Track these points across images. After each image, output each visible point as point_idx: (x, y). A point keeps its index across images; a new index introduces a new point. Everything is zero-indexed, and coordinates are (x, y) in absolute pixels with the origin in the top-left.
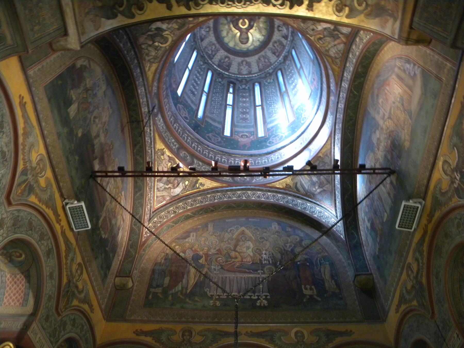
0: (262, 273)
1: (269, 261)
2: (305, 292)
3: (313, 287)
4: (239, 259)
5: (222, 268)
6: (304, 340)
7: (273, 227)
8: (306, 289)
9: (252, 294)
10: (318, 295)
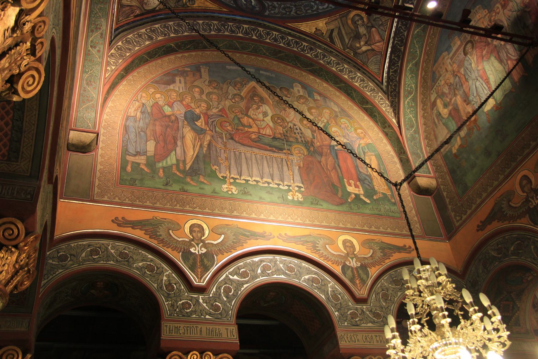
5: (232, 138)
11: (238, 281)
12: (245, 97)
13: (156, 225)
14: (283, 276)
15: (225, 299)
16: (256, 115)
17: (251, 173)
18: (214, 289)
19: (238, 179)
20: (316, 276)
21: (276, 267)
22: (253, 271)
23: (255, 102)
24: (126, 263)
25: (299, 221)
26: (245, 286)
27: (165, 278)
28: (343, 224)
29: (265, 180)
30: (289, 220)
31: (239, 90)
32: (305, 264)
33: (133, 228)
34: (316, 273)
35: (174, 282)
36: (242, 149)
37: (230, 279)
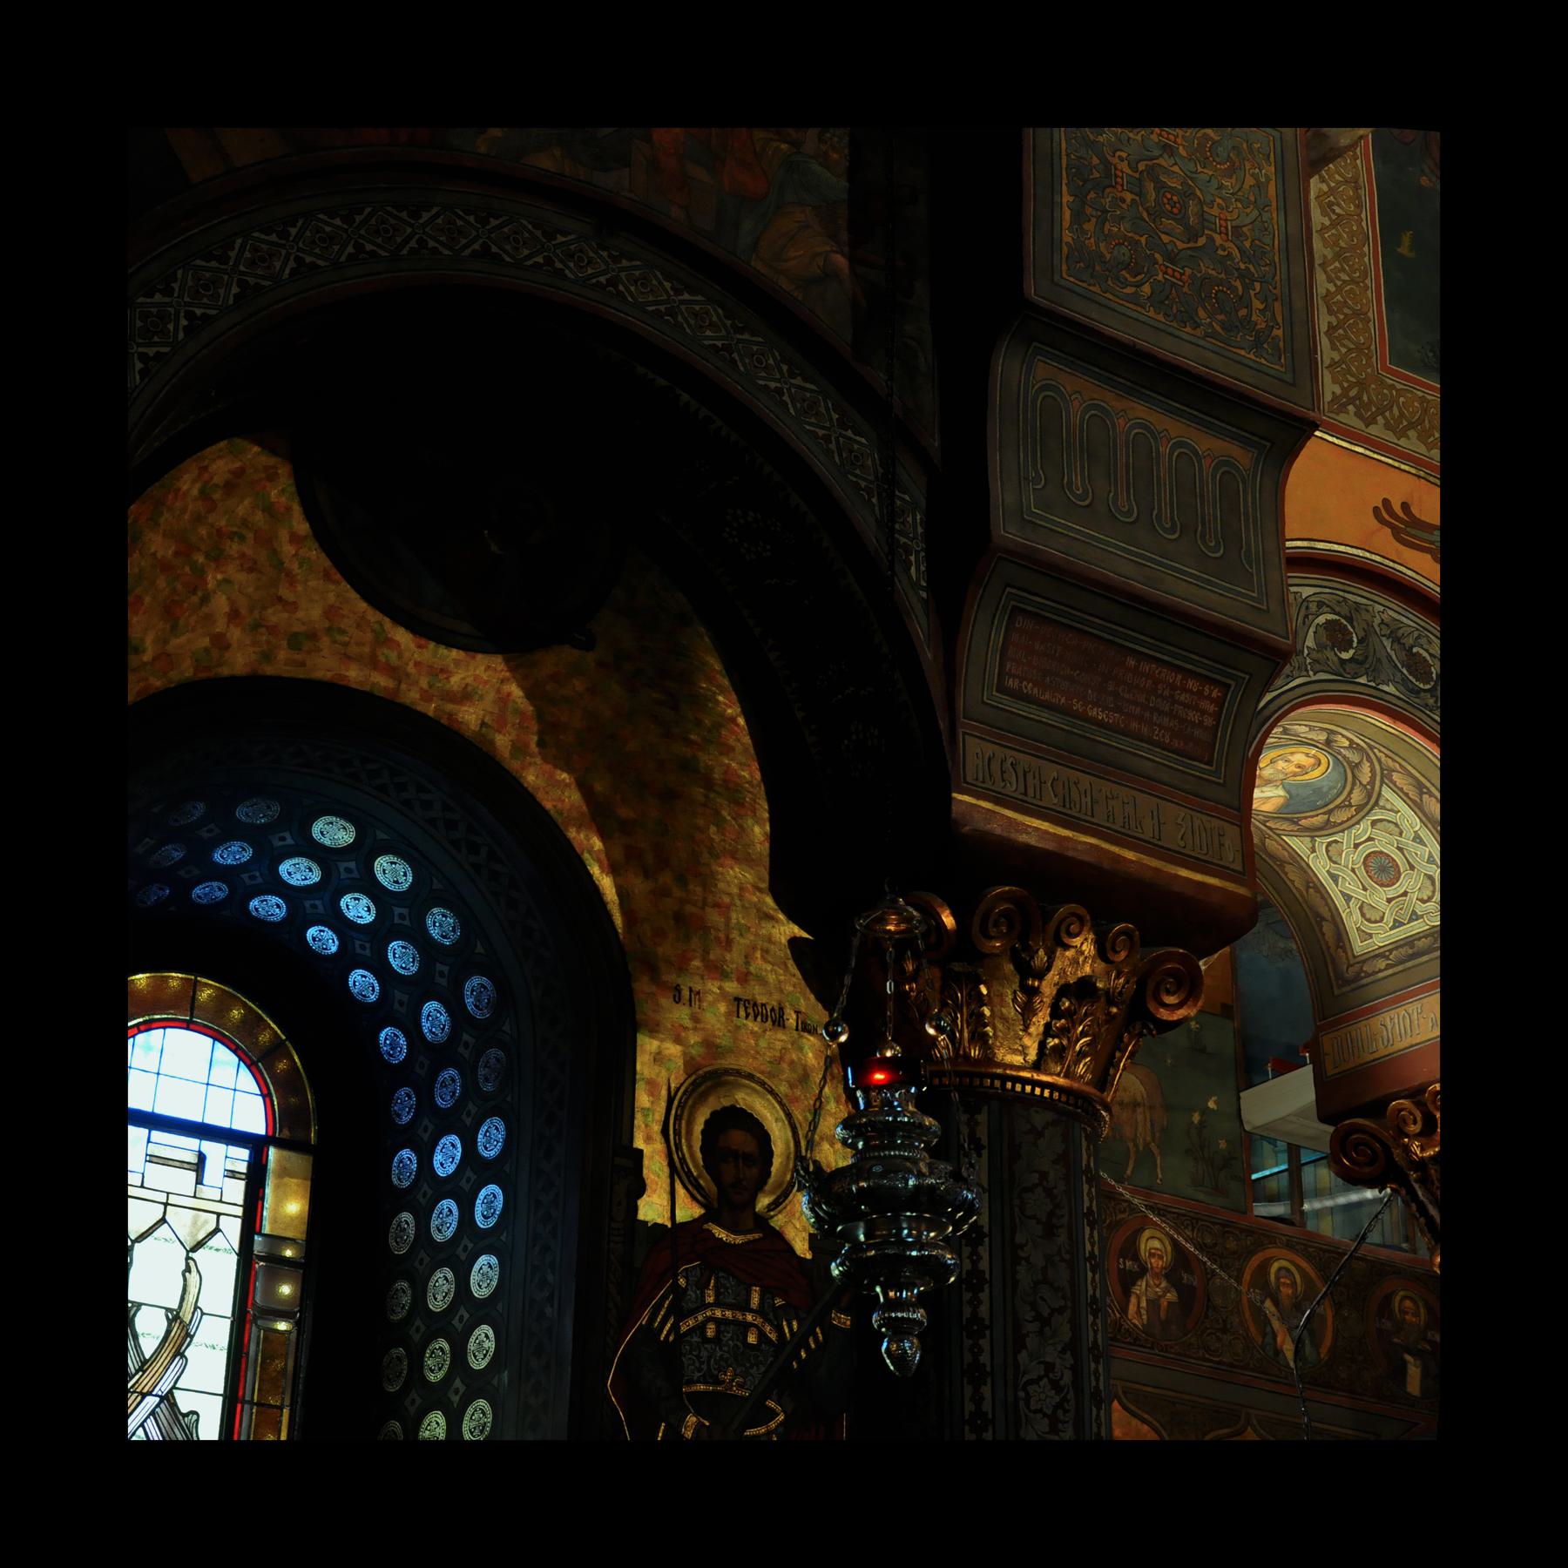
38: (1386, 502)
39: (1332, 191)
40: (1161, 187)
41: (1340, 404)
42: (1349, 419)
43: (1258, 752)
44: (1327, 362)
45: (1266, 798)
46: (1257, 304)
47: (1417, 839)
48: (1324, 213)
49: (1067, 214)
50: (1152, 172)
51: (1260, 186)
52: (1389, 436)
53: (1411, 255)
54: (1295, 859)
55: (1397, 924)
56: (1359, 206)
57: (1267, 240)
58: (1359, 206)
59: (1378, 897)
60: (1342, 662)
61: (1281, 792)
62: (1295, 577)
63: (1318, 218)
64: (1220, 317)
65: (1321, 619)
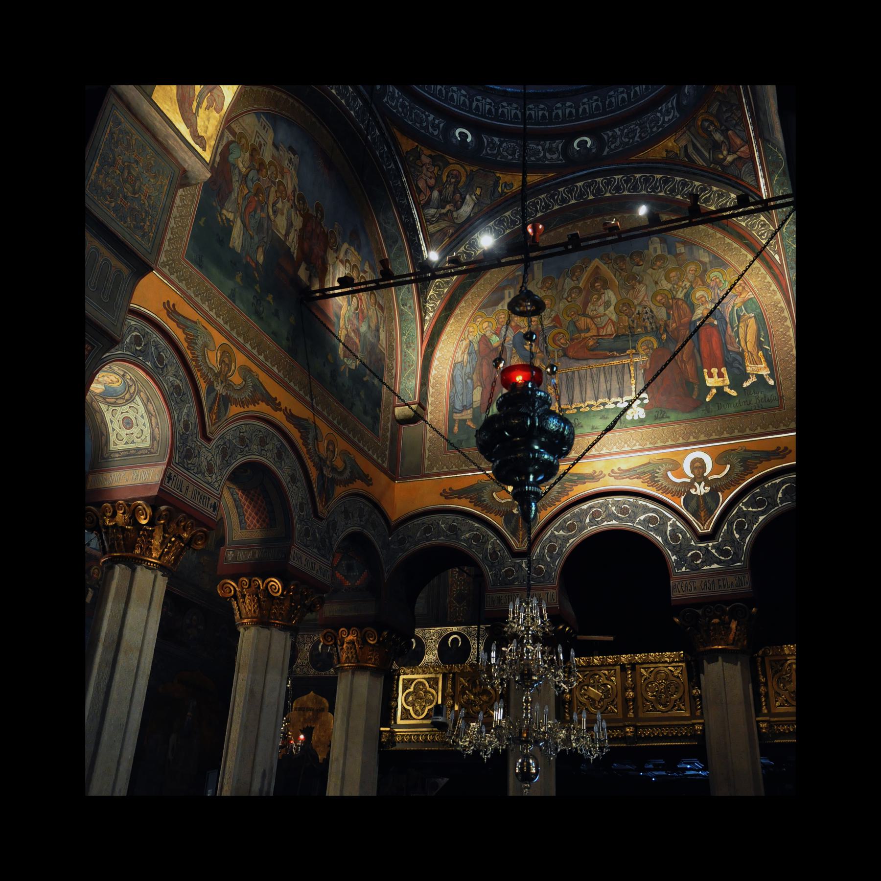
0: (633, 354)
1: (646, 328)
2: (710, 382)
3: (723, 370)
4: (593, 332)
5: (565, 355)
6: (705, 475)
7: (651, 248)
8: (711, 375)
9: (619, 399)
10: (730, 387)
11: (564, 536)
12: (584, 288)
13: (481, 489)
14: (614, 522)
15: (549, 559)
16: (595, 310)
17: (584, 396)
18: (538, 550)
19: (568, 409)
20: (654, 515)
21: (607, 512)
22: (581, 521)
23: (596, 290)
24: (455, 536)
25: (638, 447)
26: (571, 541)
27: (490, 546)
28: (694, 438)
29: (600, 401)
30: (626, 448)
31: (577, 280)
32: (641, 502)
33: (459, 498)
34: (654, 511)
35: (498, 550)
36: (575, 366)
37: (555, 536)
38: (168, 301)
39: (185, 195)
40: (130, 173)
41: (165, 264)
42: (166, 270)
43: (97, 372)
44: (165, 249)
45: (96, 387)
46: (148, 223)
47: (142, 416)
48: (181, 202)
49: (95, 170)
50: (128, 166)
51: (162, 186)
52: (176, 281)
53: (202, 225)
54: (101, 412)
55: (127, 443)
56: (192, 204)
57: (158, 203)
58: (192, 204)
59: (124, 432)
60: (136, 350)
61: (103, 388)
62: (130, 316)
63: (178, 201)
64: (134, 223)
65: (134, 334)
